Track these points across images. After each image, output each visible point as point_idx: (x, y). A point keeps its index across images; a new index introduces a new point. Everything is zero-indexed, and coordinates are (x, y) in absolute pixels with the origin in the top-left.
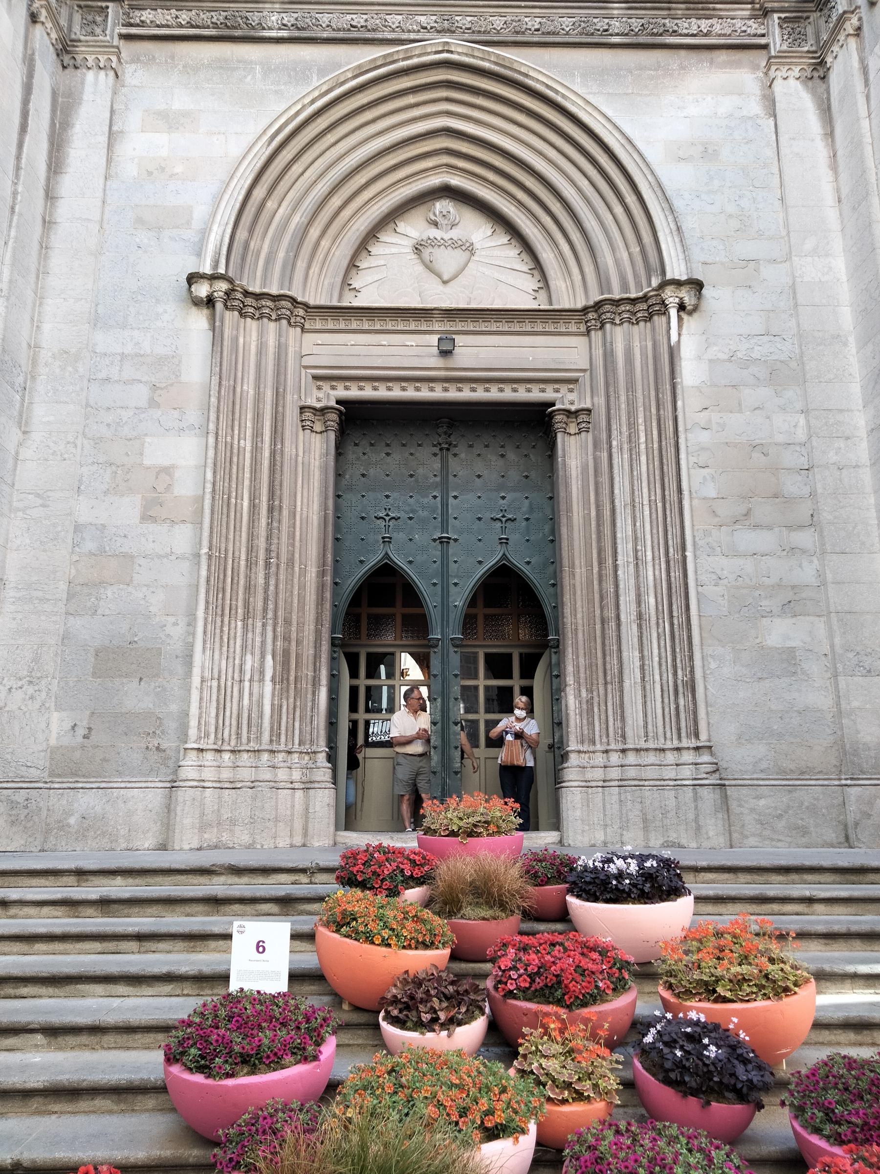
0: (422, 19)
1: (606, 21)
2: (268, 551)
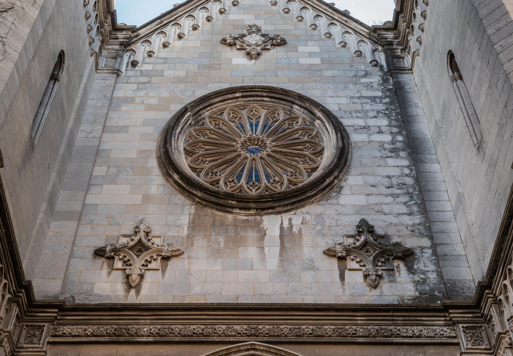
0: (238, 327)
1: (354, 327)
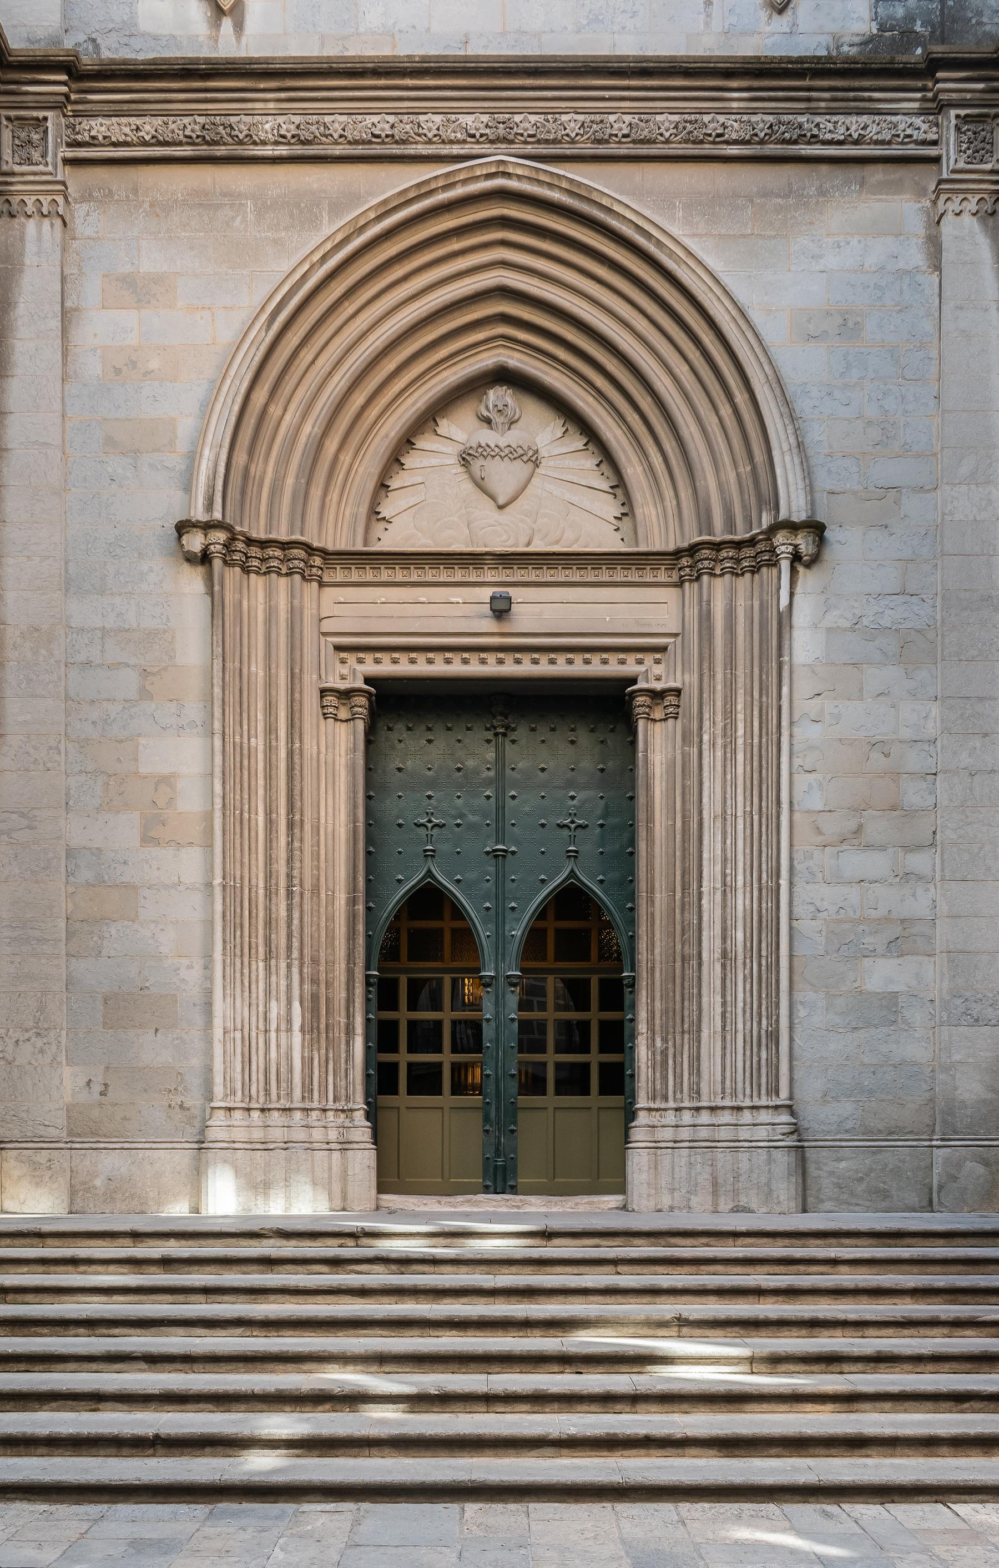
0: (467, 120)
1: (721, 118)
2: (290, 877)
